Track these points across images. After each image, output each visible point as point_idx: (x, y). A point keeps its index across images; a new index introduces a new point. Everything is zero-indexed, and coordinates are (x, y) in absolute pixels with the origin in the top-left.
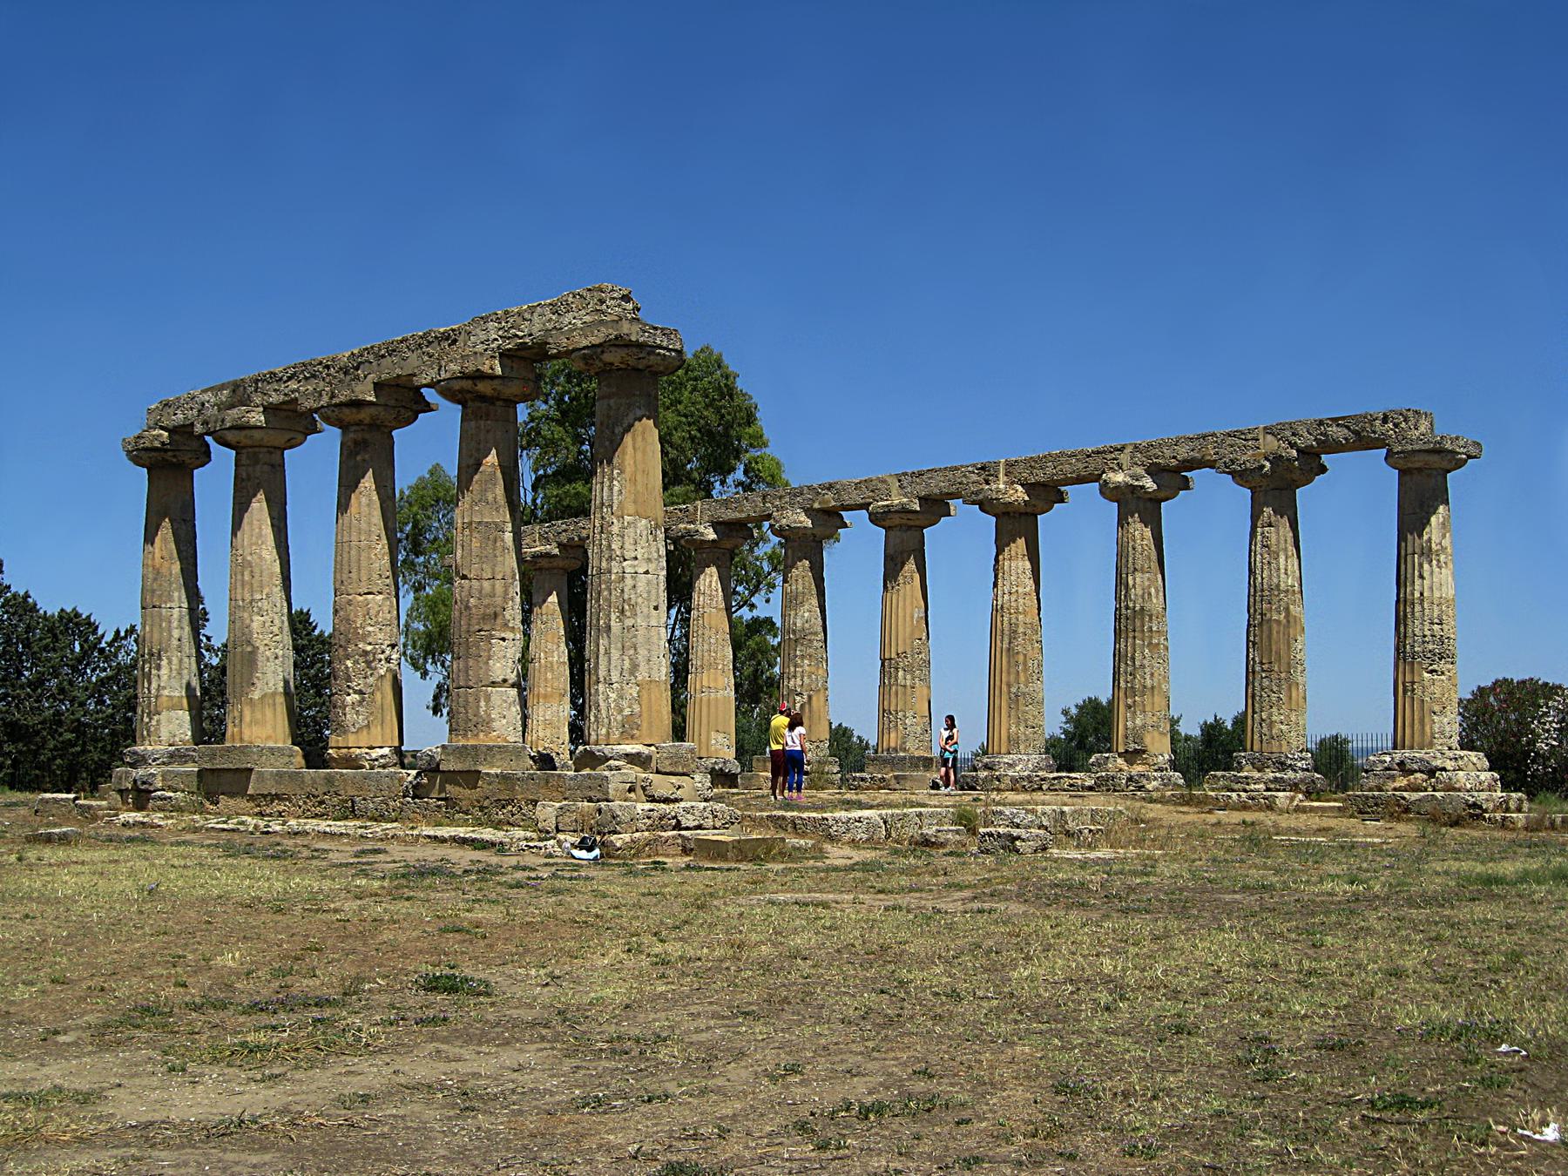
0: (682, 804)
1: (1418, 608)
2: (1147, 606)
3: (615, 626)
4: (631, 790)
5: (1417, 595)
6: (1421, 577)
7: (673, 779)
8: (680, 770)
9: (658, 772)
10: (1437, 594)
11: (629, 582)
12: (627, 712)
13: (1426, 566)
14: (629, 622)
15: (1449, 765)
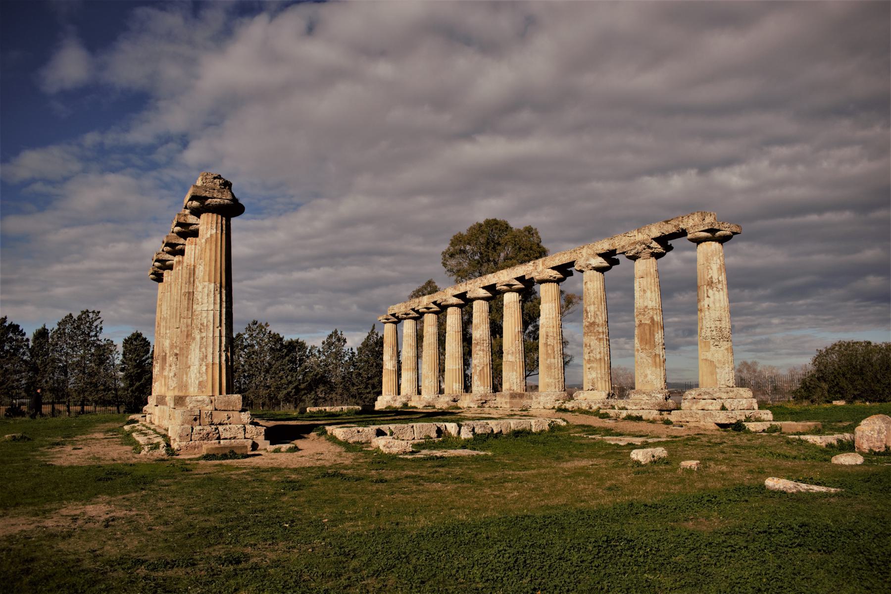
0: (224, 427)
1: (707, 313)
2: (597, 321)
3: (198, 337)
4: (195, 420)
5: (706, 306)
6: (708, 297)
7: (225, 414)
8: (231, 408)
9: (216, 410)
10: (718, 305)
11: (205, 315)
12: (201, 379)
13: (710, 291)
14: (204, 334)
15: (724, 396)
